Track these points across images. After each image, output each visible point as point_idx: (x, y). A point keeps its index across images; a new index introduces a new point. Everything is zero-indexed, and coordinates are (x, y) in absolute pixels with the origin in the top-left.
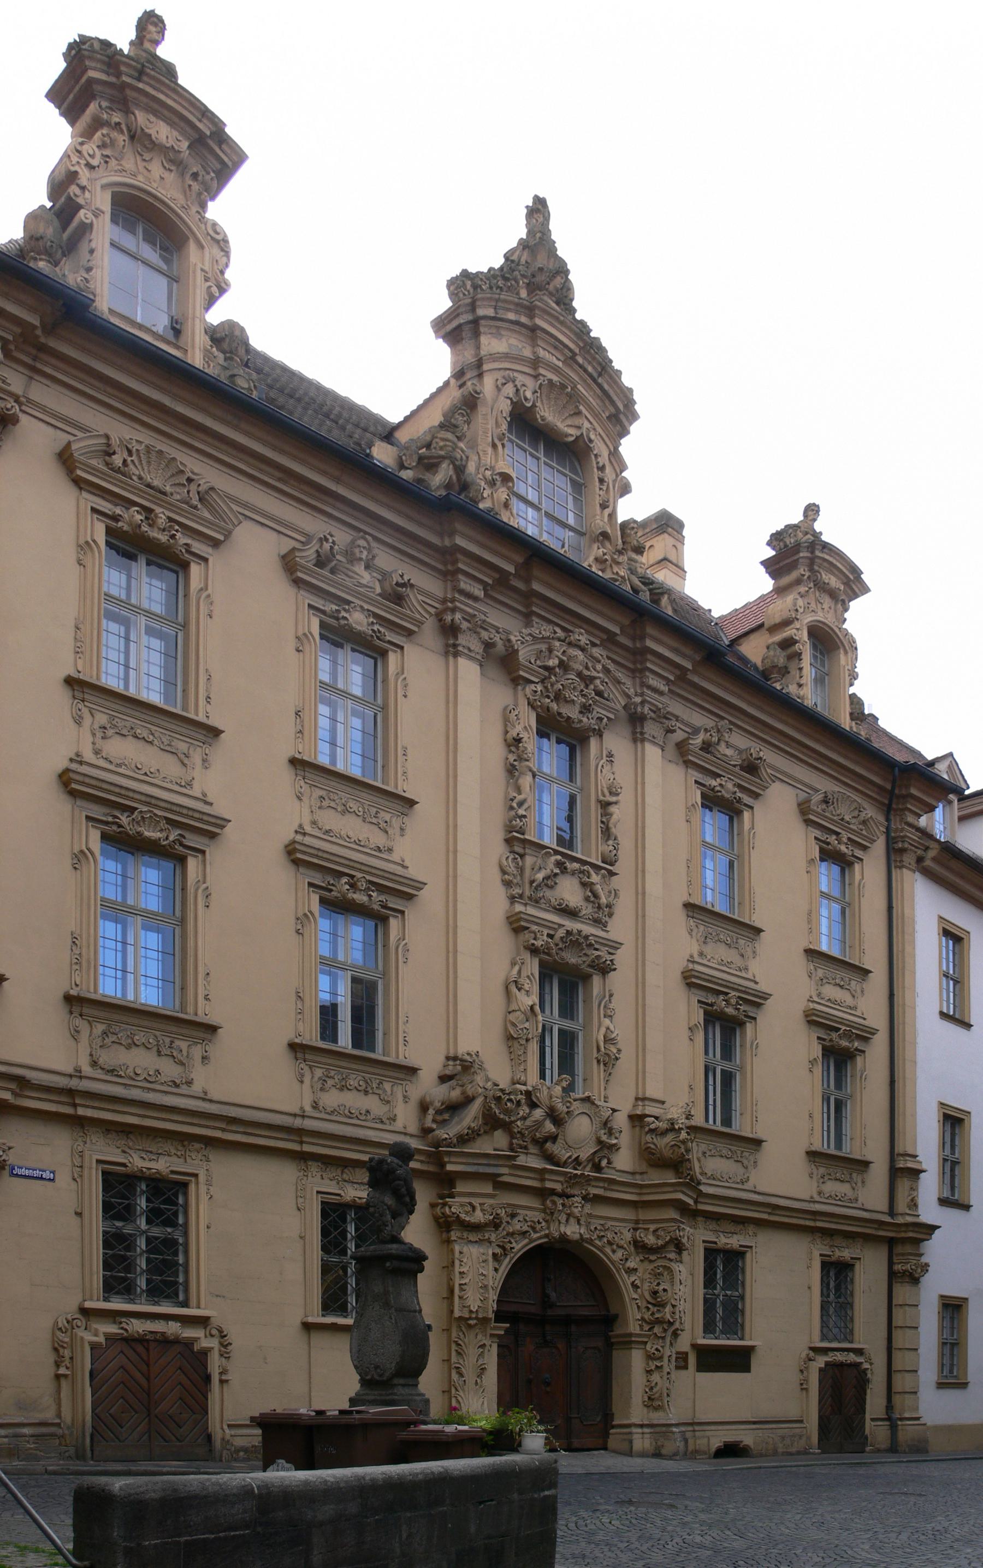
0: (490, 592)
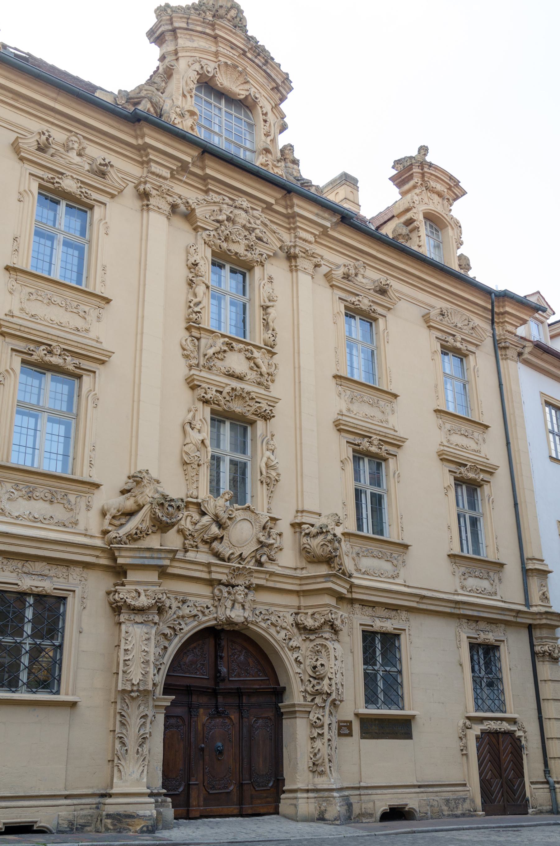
0: (177, 176)
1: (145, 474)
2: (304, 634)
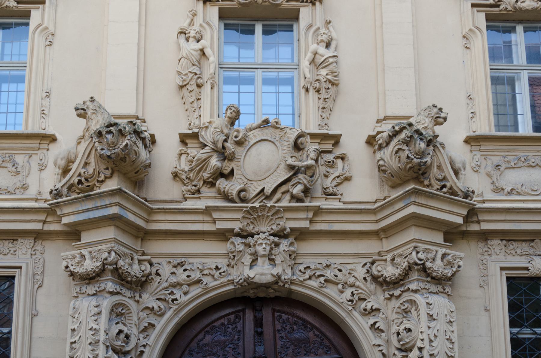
2: (389, 290)
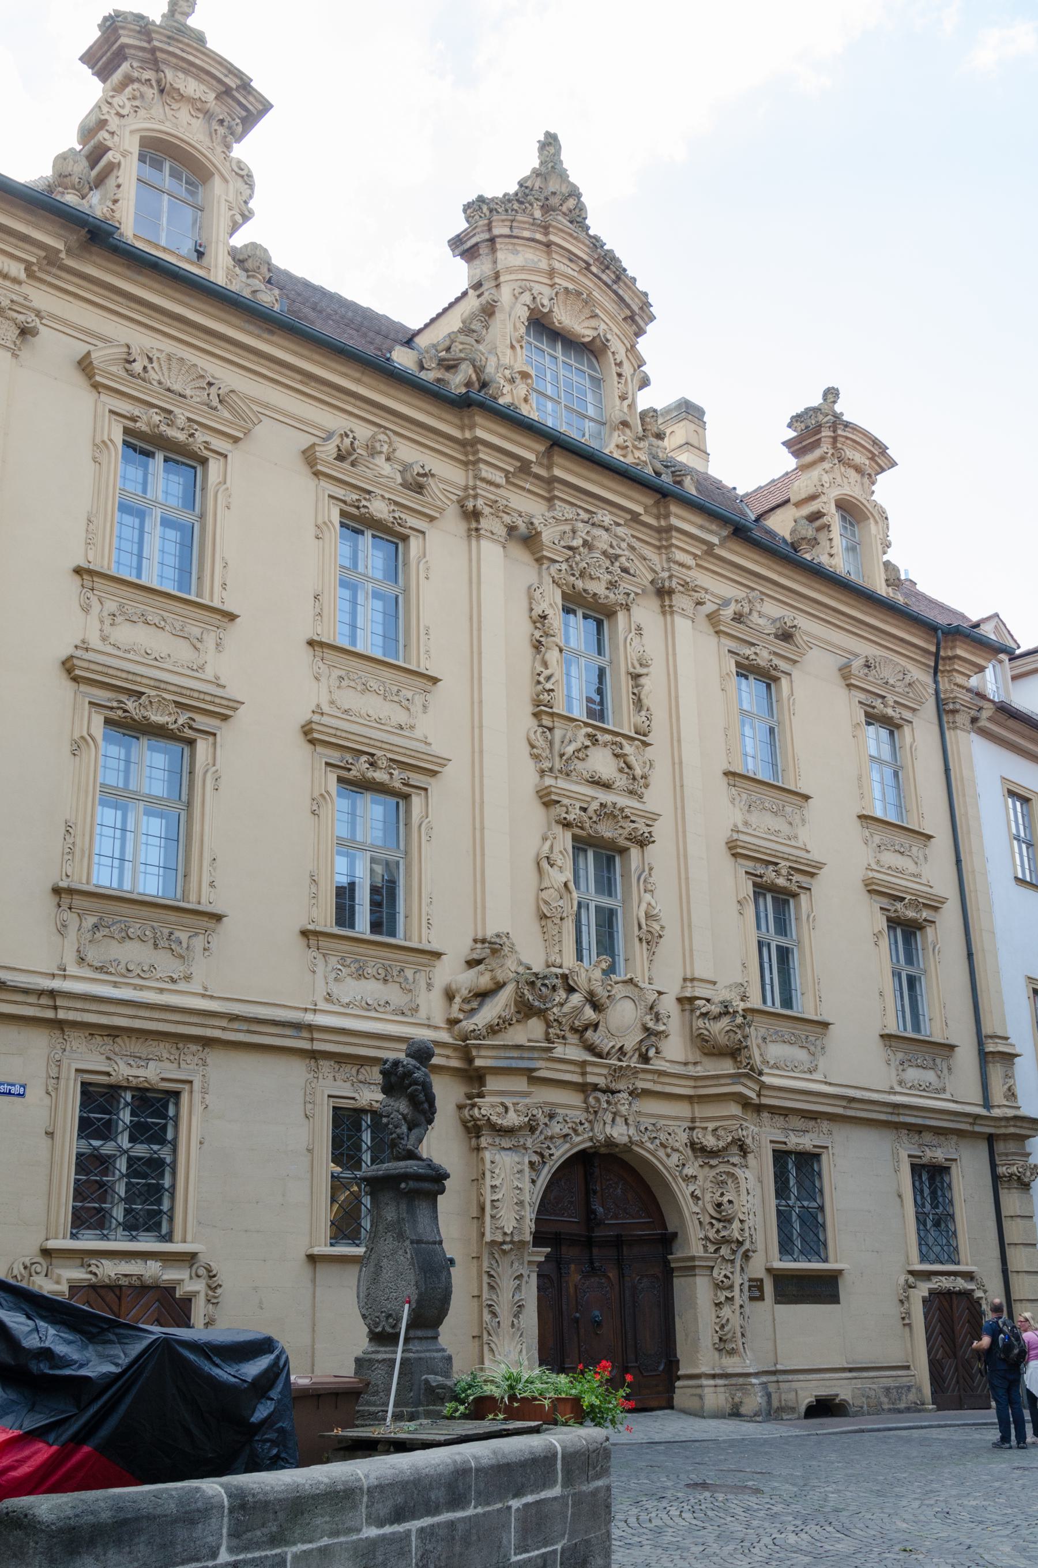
1: (505, 939)
